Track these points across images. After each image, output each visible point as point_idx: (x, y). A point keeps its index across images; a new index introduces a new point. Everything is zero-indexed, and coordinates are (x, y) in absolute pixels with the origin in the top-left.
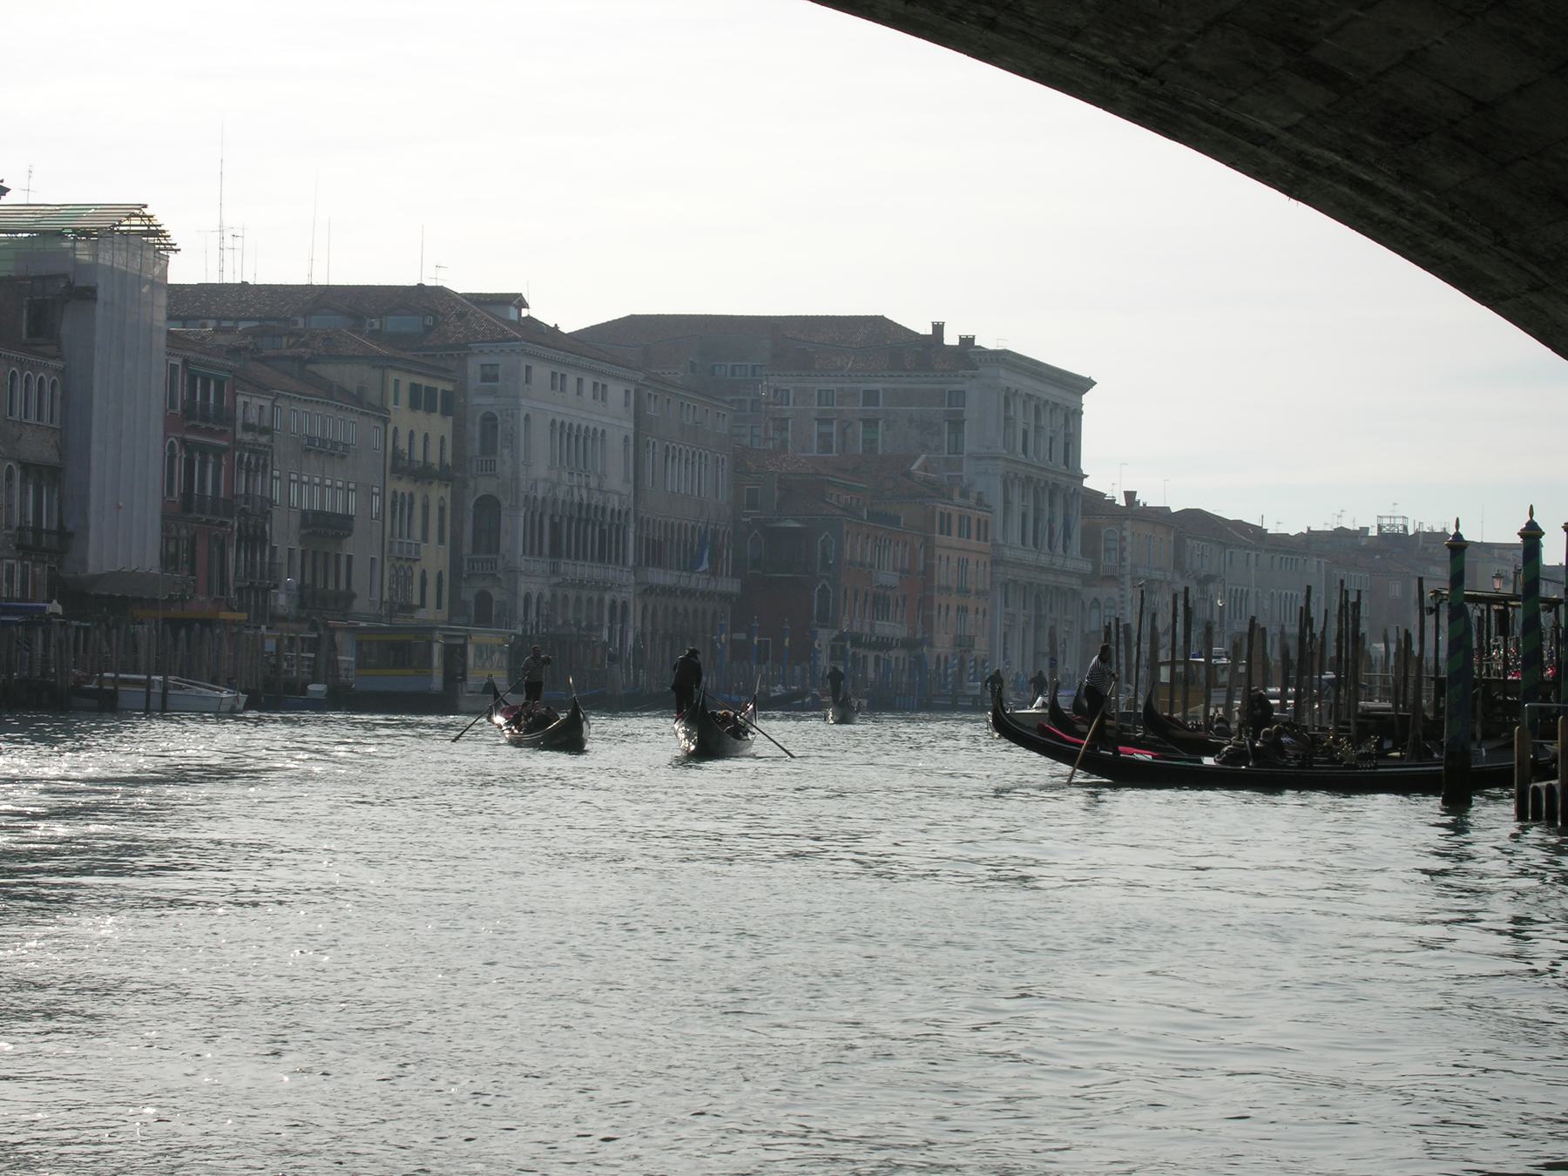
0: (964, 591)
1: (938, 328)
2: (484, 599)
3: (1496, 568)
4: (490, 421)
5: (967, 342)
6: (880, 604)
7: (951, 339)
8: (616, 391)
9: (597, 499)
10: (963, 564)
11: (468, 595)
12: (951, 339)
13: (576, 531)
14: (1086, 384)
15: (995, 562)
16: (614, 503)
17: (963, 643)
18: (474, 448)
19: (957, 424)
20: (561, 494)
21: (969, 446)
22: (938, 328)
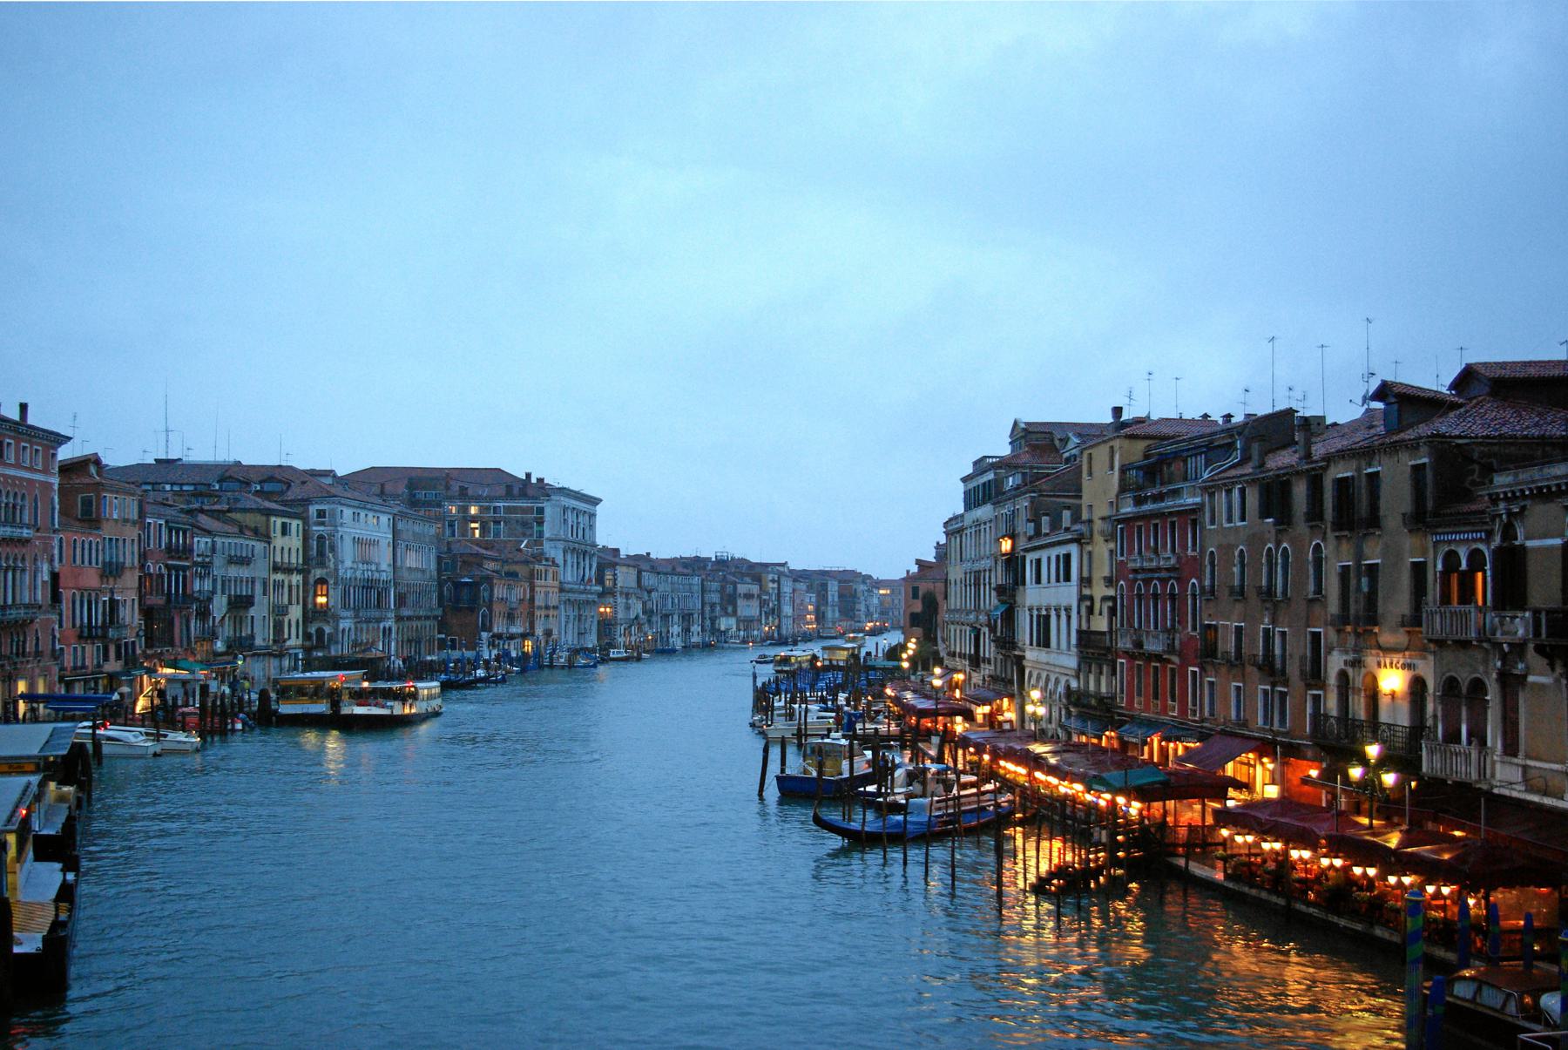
0: (547, 608)
1: (528, 475)
2: (320, 632)
3: (770, 577)
4: (321, 537)
5: (540, 480)
6: (511, 617)
7: (534, 480)
8: (384, 519)
9: (376, 575)
10: (547, 594)
11: (312, 630)
12: (534, 480)
13: (369, 594)
14: (595, 501)
15: (561, 590)
16: (384, 576)
17: (548, 633)
18: (314, 552)
19: (541, 522)
20: (358, 574)
21: (547, 534)
22: (528, 475)
